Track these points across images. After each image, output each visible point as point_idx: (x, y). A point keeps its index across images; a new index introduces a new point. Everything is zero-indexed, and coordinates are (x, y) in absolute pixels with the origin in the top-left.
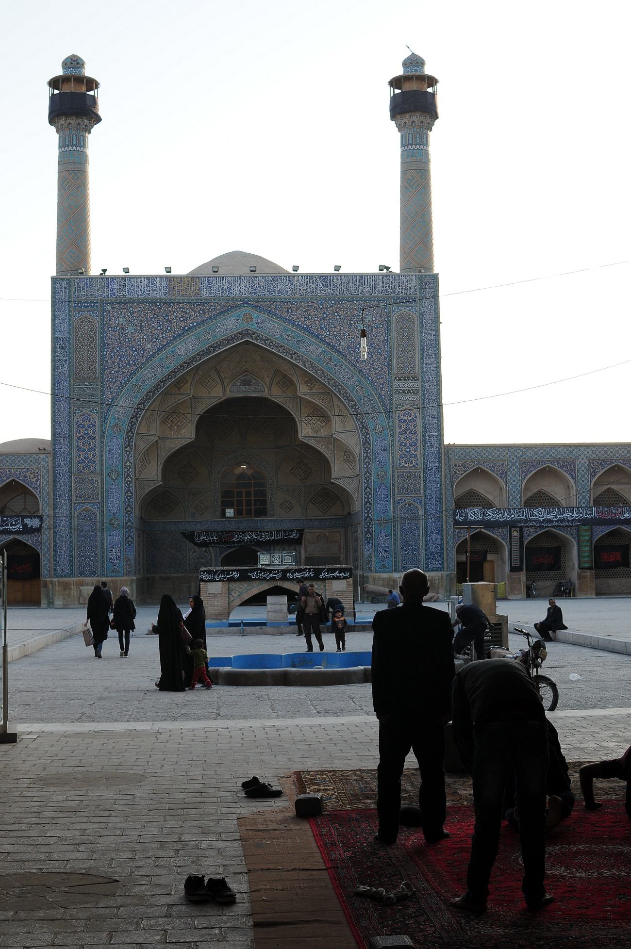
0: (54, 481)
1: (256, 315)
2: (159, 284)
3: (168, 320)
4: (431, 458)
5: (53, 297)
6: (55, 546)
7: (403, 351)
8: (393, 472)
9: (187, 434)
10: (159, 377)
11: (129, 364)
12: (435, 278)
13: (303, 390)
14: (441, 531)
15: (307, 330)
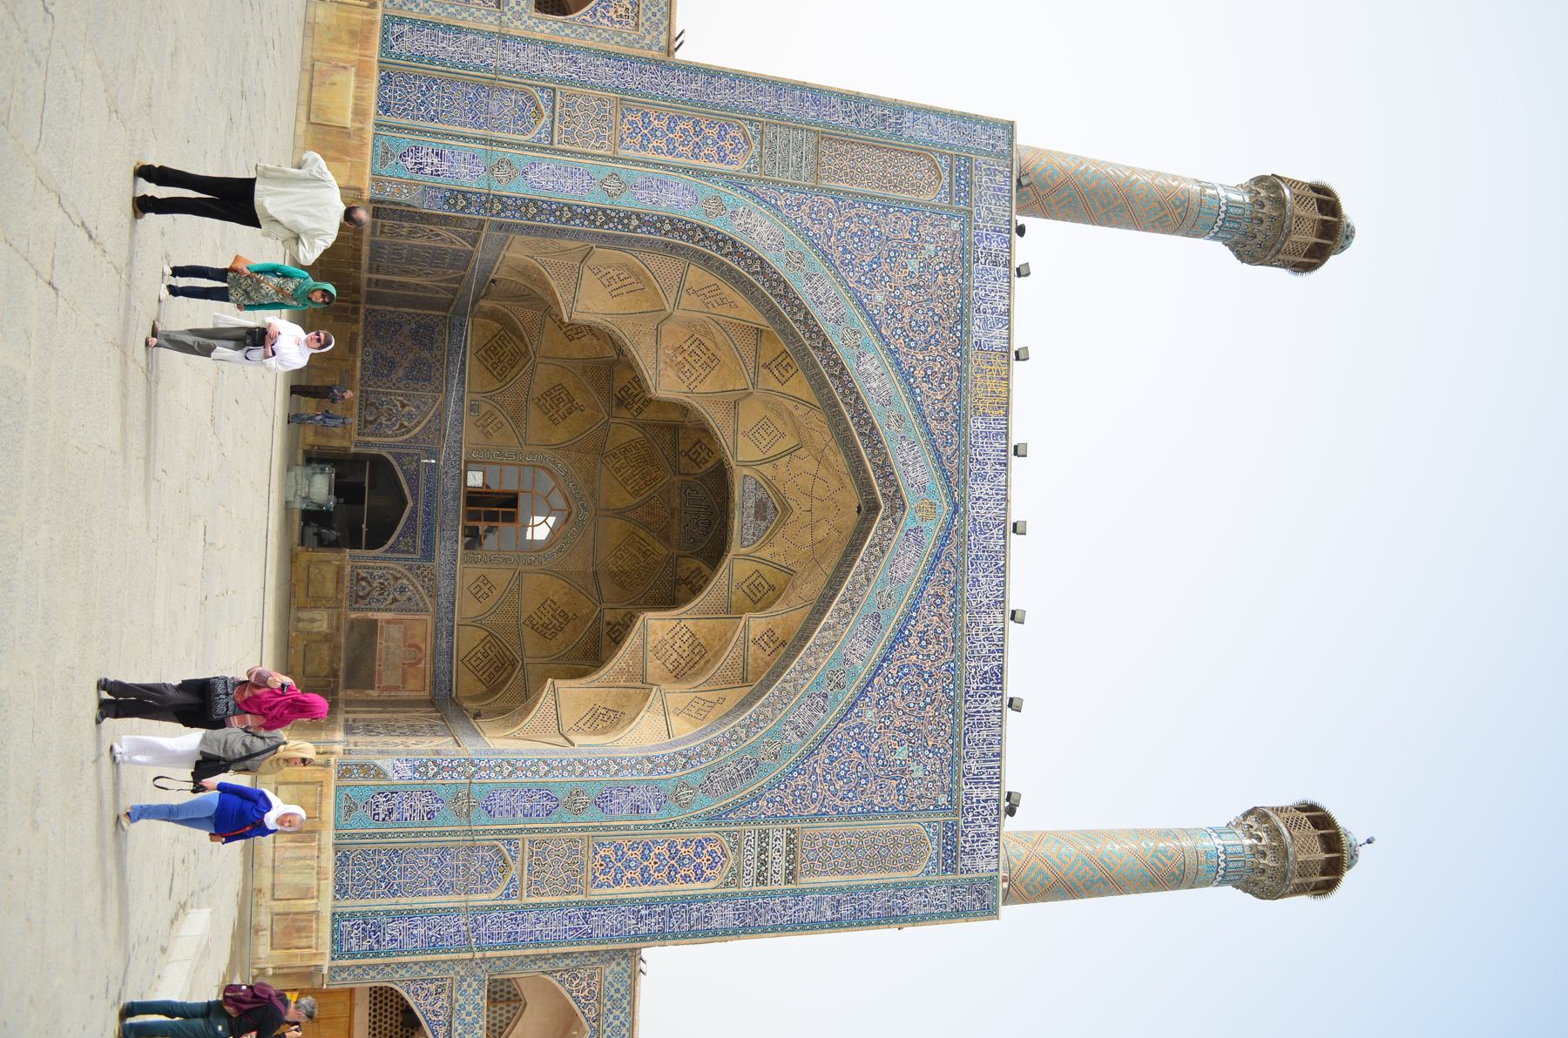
0: (607, 55)
1: (932, 530)
2: (996, 332)
3: (928, 343)
4: (612, 919)
5: (976, 120)
6: (459, 30)
7: (849, 847)
8: (585, 829)
9: (665, 383)
10: (816, 312)
11: (845, 251)
12: (990, 912)
13: (757, 624)
14: (434, 948)
15: (900, 637)
